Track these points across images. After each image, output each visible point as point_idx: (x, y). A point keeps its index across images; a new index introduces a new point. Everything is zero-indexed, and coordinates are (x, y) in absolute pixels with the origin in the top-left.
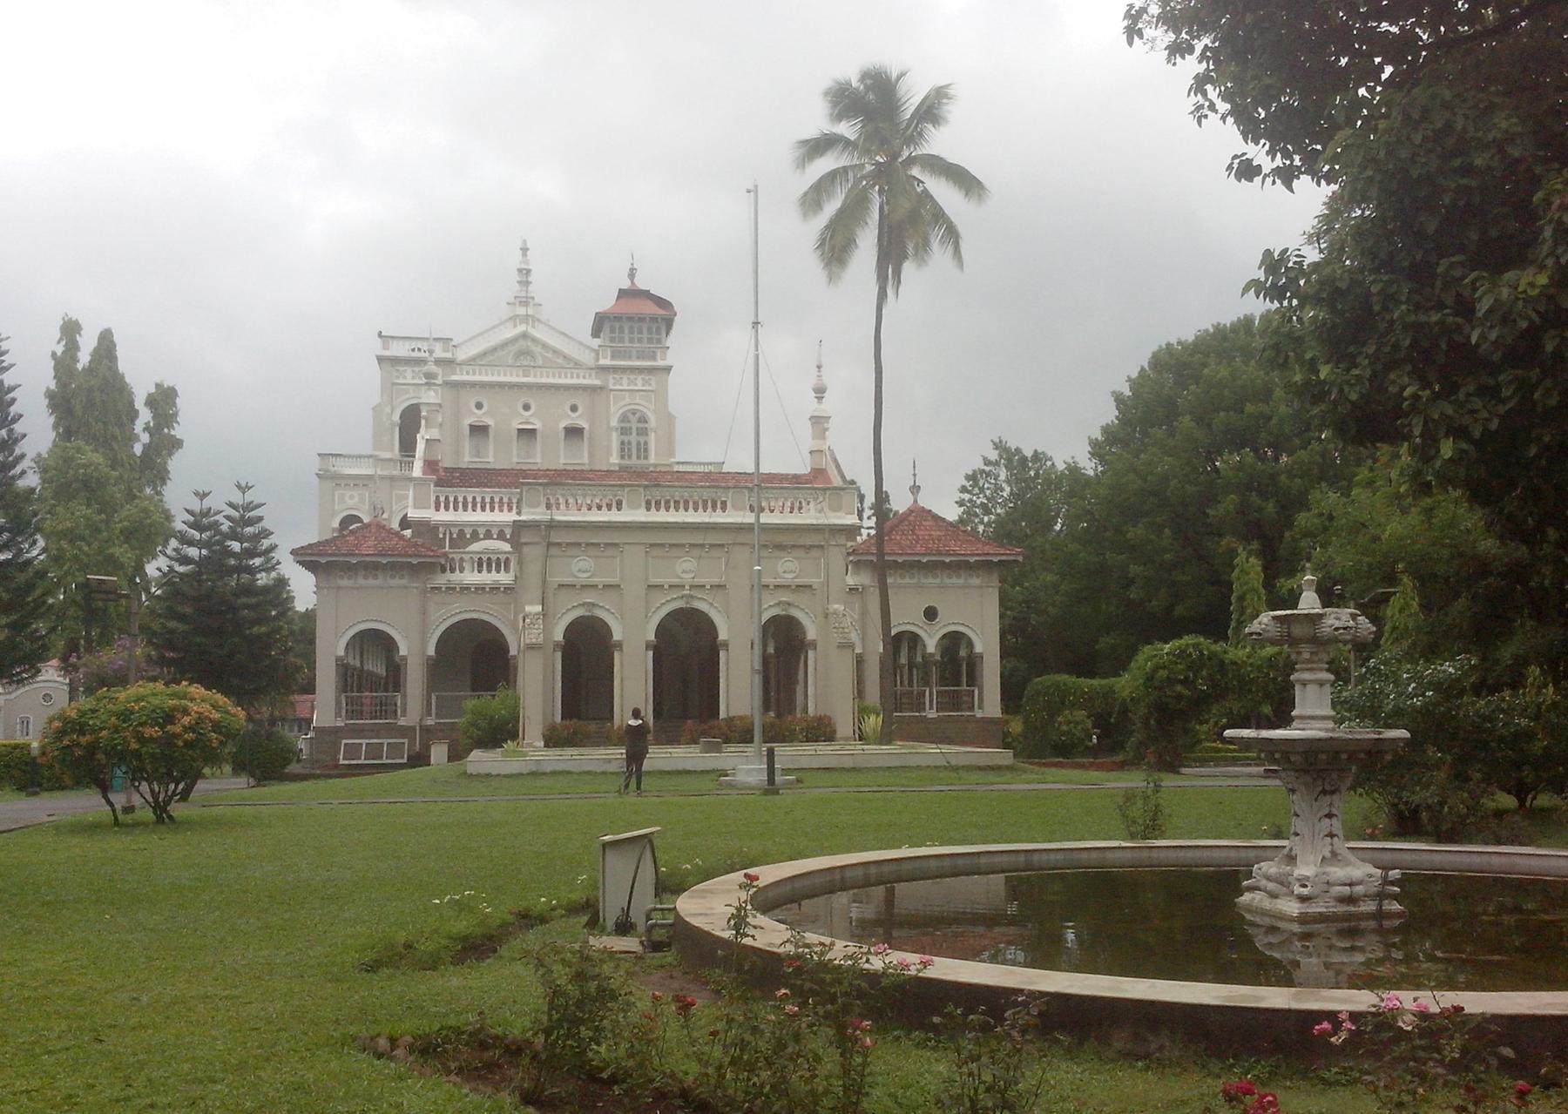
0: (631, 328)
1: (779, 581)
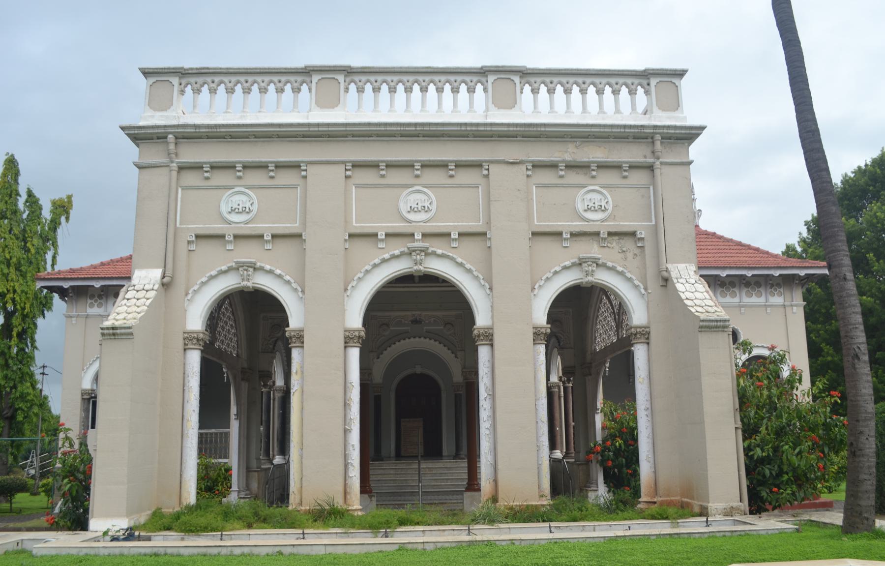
1: (578, 225)
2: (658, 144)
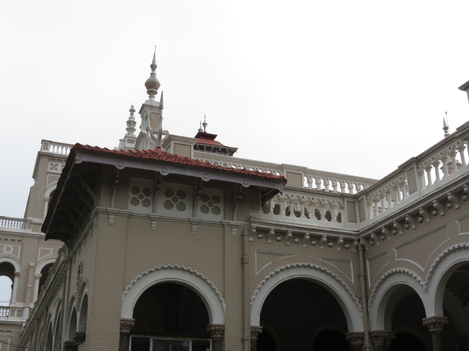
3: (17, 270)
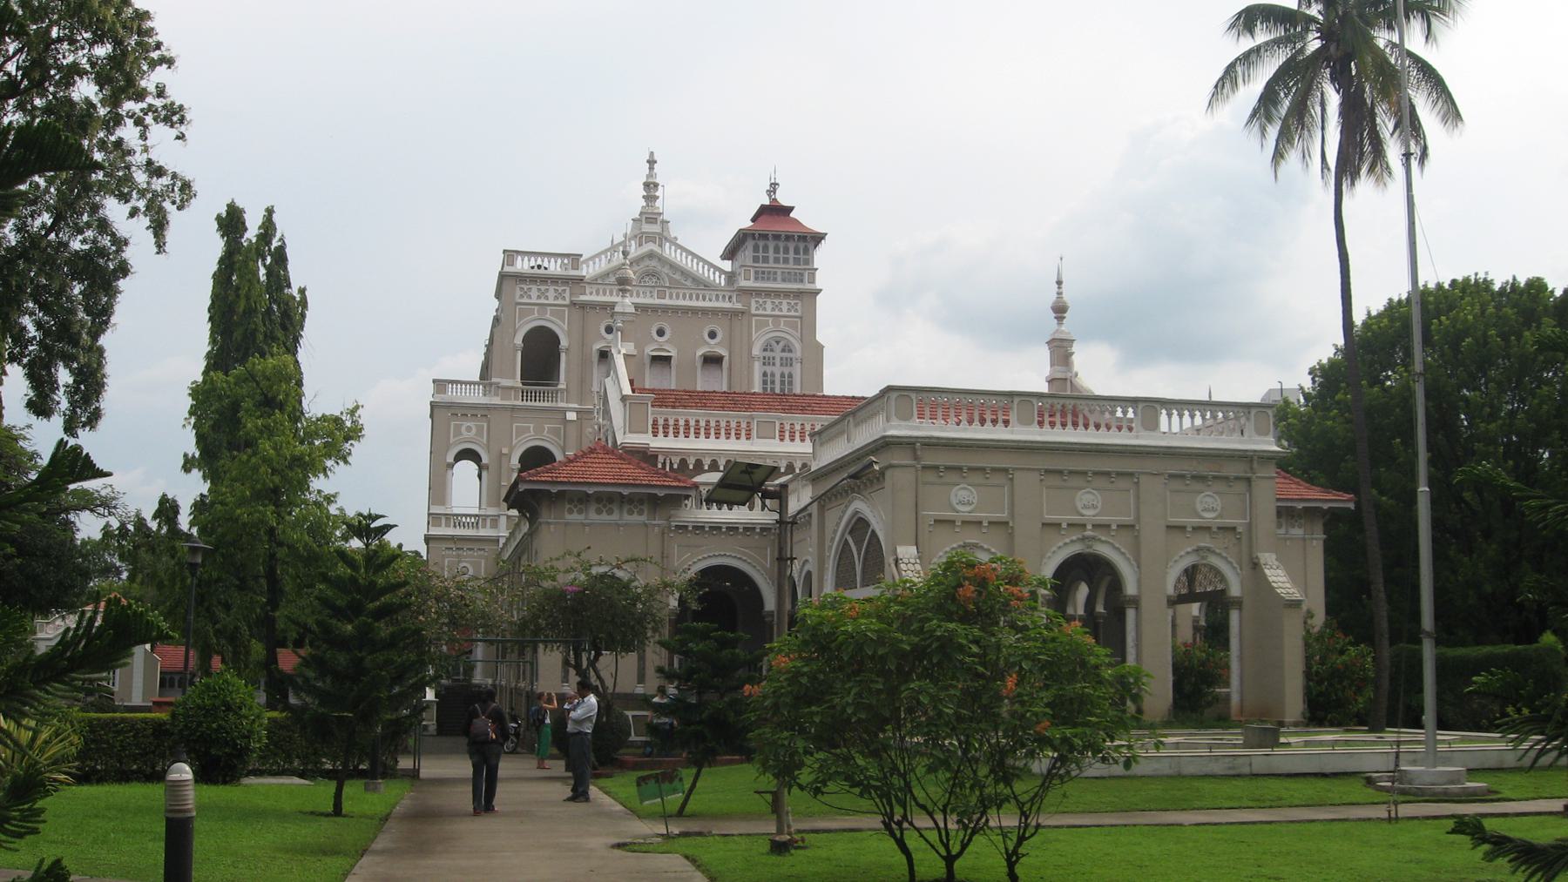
0: (777, 250)
2: (1255, 465)
3: (485, 460)
